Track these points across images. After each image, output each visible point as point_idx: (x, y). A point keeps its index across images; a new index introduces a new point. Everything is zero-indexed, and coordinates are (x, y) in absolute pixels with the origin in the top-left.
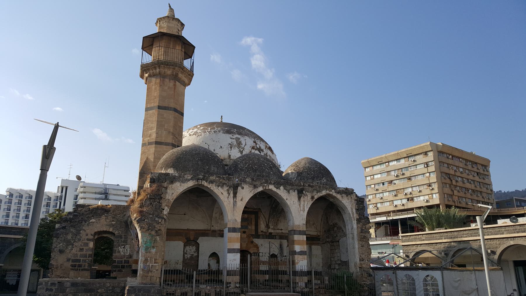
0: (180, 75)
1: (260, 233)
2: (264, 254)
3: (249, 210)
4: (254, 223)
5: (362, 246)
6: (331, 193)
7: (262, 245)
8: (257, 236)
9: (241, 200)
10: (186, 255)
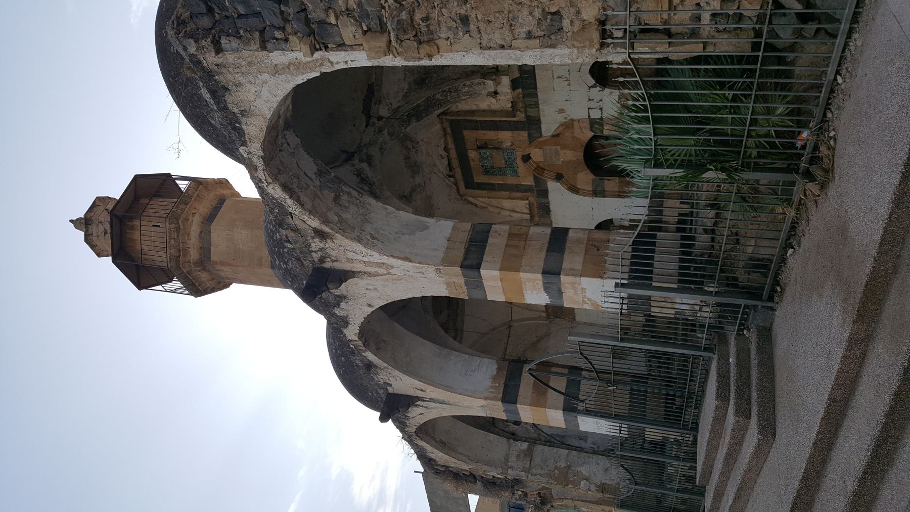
1: (520, 117)
2: (593, 104)
3: (451, 146)
4: (490, 135)
5: (465, 20)
7: (561, 111)
8: (533, 124)
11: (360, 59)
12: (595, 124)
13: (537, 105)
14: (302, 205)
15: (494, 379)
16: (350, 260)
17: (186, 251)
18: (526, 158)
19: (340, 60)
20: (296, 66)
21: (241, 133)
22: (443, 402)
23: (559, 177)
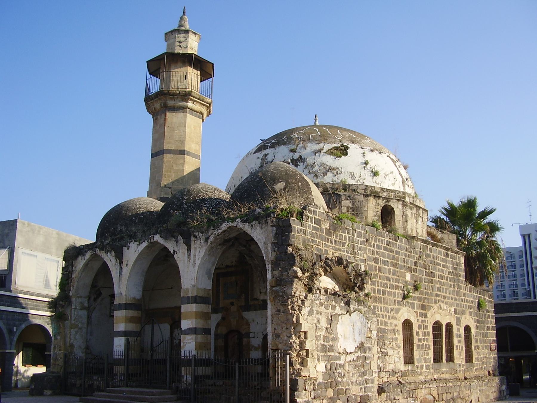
0: (170, 103)
1: (251, 303)
6: (234, 224)
7: (253, 321)
8: (247, 308)
9: (127, 265)
10: (175, 341)
11: (269, 276)
12: (248, 335)
13: (256, 310)
14: (218, 235)
15: (134, 298)
16: (195, 248)
17: (172, 99)
18: (232, 304)
19: (269, 267)
20: (267, 253)
21: (245, 222)
22: (121, 274)
23: (223, 318)
